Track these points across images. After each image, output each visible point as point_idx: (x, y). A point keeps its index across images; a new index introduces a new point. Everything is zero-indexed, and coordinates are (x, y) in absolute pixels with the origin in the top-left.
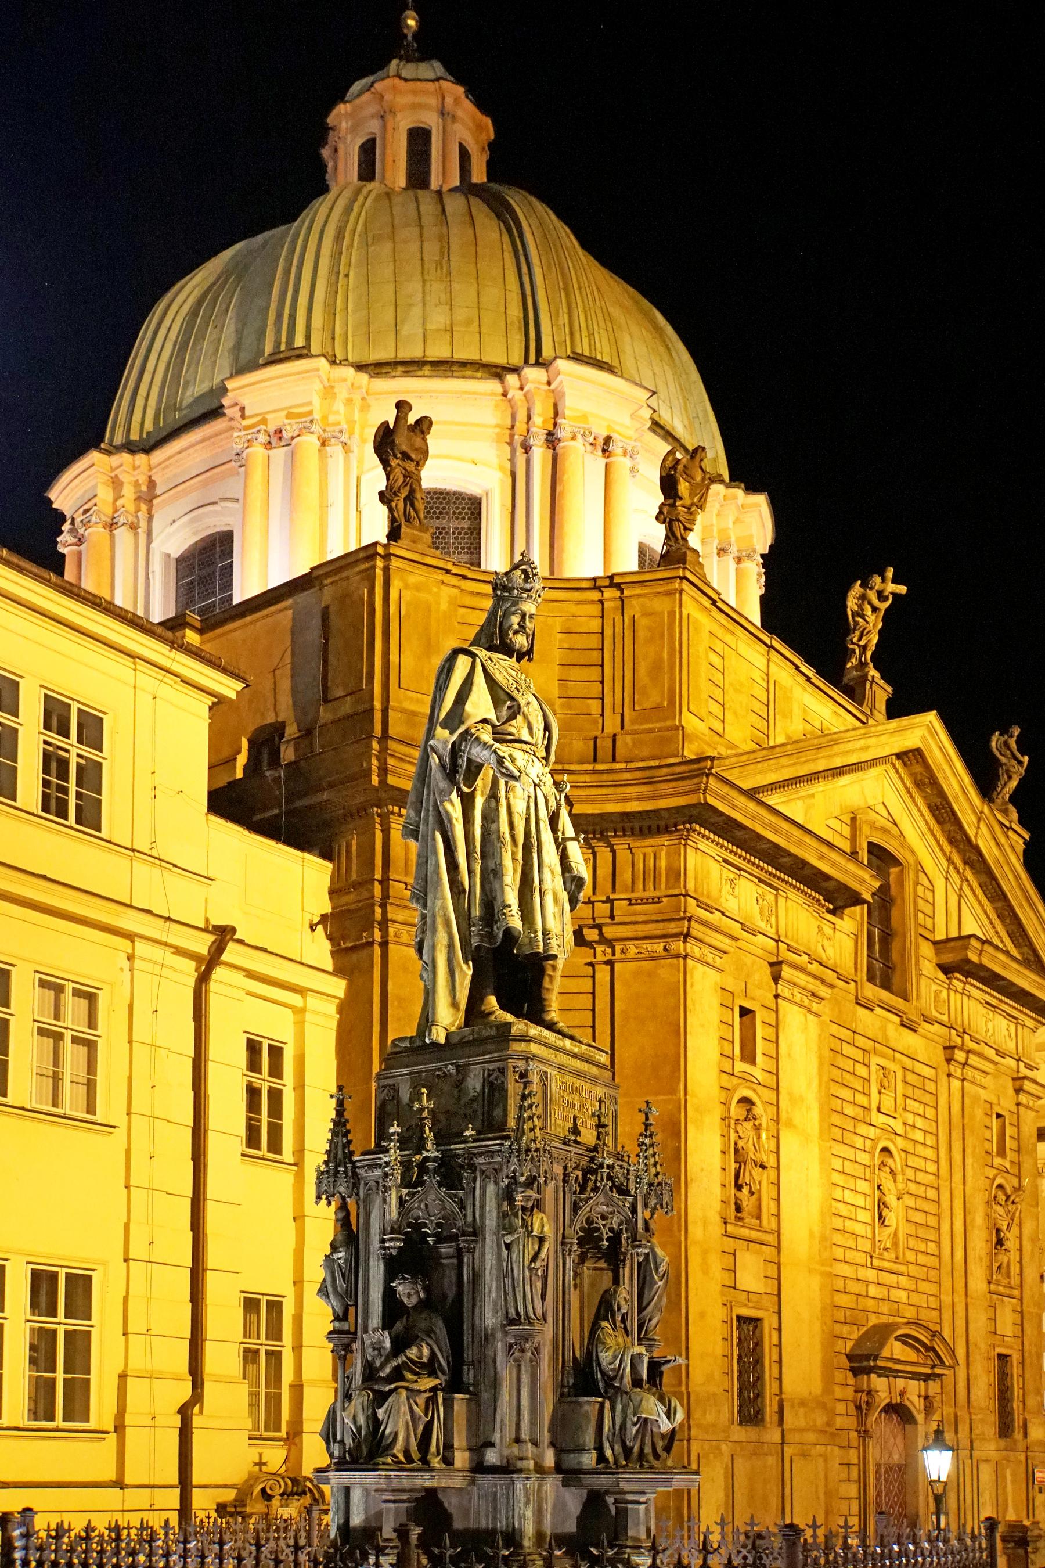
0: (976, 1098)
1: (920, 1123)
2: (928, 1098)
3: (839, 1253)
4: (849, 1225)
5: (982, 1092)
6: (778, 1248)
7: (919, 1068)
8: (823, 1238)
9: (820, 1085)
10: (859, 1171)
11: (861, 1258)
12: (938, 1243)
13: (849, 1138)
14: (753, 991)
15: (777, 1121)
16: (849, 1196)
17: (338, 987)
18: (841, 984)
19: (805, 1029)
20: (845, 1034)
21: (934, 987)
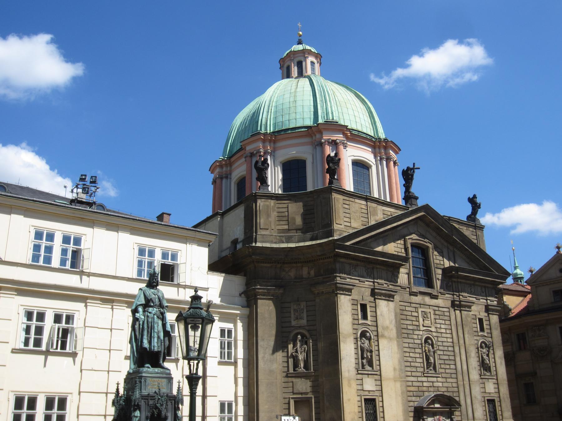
0: (467, 316)
1: (443, 326)
2: (446, 318)
3: (409, 374)
4: (413, 364)
6: (380, 375)
8: (401, 370)
9: (396, 322)
10: (416, 346)
11: (419, 374)
12: (455, 365)
13: (410, 336)
14: (365, 298)
15: (377, 336)
16: (411, 355)
17: (246, 311)
19: (388, 306)
20: (409, 304)
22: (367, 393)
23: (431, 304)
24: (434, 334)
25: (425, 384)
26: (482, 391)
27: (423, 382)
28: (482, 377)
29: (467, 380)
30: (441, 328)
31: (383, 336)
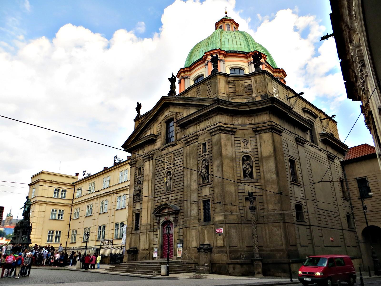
1: (178, 161)
2: (181, 155)
5: (196, 143)
7: (178, 151)
12: (183, 183)
18: (158, 151)
21: (182, 132)
22: (137, 211)
23: (173, 150)
24: (173, 168)
25: (164, 200)
26: (200, 195)
27: (163, 199)
28: (200, 185)
29: (189, 190)
30: (177, 163)
31: (145, 180)
